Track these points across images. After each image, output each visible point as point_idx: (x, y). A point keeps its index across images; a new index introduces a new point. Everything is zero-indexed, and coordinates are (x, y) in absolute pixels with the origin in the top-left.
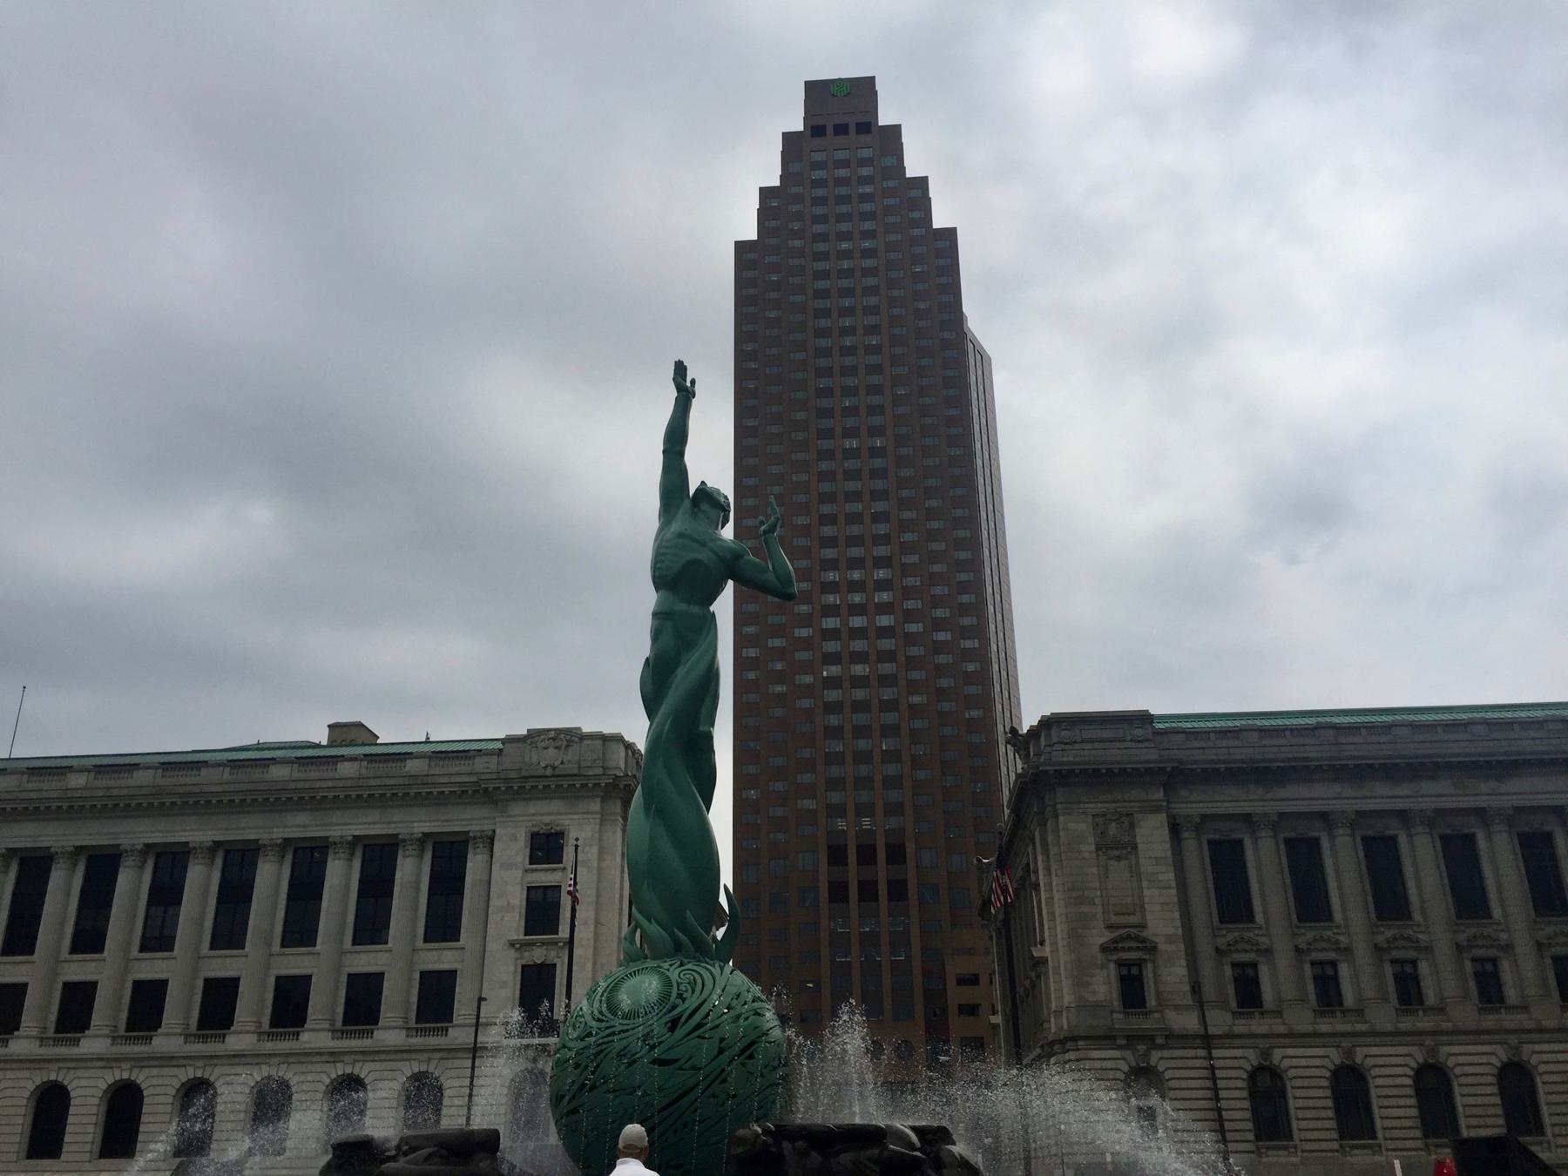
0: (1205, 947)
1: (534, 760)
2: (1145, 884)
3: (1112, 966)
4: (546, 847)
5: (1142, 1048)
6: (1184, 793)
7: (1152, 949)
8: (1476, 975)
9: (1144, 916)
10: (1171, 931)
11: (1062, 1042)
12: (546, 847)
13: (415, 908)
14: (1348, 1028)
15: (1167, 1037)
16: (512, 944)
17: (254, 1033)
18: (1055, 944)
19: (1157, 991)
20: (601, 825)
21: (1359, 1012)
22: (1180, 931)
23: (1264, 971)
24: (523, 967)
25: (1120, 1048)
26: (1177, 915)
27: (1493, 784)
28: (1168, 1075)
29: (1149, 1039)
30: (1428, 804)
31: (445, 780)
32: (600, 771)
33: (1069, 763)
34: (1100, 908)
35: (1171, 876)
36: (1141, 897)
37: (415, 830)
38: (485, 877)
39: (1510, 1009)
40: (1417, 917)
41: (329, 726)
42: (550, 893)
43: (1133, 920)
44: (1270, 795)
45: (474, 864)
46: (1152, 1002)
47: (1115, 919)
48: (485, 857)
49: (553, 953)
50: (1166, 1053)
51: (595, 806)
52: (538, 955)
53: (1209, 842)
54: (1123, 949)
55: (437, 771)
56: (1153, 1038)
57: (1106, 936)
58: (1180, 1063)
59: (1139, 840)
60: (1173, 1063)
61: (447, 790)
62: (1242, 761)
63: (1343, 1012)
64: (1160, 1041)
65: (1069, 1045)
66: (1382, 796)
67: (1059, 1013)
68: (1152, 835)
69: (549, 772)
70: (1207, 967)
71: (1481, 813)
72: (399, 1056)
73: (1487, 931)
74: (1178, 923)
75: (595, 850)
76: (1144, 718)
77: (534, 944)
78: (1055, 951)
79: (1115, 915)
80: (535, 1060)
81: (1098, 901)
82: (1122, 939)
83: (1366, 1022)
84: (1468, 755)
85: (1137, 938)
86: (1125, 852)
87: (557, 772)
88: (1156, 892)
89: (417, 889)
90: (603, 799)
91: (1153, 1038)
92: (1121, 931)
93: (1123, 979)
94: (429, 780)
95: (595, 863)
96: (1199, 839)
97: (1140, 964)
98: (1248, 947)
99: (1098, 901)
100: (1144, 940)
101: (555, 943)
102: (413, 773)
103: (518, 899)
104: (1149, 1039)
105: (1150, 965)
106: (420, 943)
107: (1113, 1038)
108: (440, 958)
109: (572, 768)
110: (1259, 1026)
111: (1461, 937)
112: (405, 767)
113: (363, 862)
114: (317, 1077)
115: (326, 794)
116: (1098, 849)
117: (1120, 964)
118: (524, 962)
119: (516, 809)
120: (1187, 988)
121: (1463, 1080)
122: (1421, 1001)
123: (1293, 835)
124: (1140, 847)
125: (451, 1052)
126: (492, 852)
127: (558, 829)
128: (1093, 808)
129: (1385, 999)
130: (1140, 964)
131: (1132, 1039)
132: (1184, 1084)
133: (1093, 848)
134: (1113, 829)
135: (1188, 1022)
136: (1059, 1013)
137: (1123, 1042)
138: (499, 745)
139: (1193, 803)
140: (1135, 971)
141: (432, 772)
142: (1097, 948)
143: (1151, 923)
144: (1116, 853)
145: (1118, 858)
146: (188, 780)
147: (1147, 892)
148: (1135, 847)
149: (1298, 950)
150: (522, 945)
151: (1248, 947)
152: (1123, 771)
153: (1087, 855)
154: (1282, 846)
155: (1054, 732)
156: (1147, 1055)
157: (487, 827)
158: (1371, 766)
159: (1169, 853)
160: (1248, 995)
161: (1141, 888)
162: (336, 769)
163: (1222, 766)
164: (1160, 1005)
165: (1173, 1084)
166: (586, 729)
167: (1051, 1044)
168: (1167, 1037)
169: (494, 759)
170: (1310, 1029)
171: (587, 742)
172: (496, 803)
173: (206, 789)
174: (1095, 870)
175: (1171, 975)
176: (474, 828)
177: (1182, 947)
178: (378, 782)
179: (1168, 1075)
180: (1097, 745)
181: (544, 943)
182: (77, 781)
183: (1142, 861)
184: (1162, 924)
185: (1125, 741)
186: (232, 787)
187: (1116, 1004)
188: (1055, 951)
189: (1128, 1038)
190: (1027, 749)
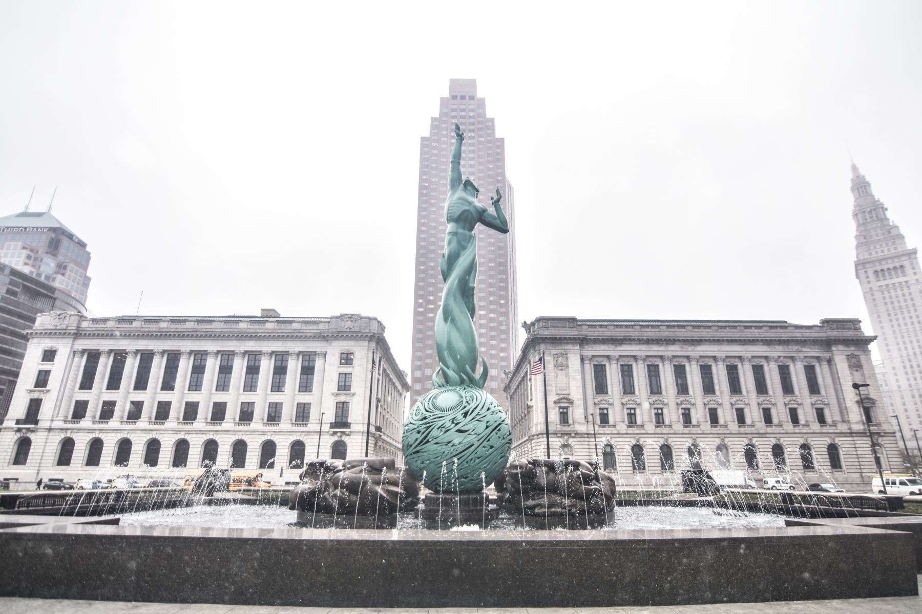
0: (590, 403)
1: (343, 325)
2: (571, 379)
3: (557, 408)
4: (347, 359)
5: (566, 437)
6: (586, 347)
7: (572, 403)
8: (683, 414)
9: (570, 392)
10: (579, 397)
11: (538, 435)
12: (347, 359)
13: (295, 379)
14: (638, 432)
15: (576, 434)
16: (333, 394)
18: (537, 400)
19: (573, 418)
20: (368, 351)
21: (642, 426)
22: (582, 397)
23: (610, 411)
24: (337, 403)
25: (559, 437)
26: (581, 391)
27: (693, 347)
28: (575, 447)
29: (569, 434)
30: (670, 354)
31: (308, 331)
32: (367, 331)
33: (546, 335)
34: (554, 388)
35: (580, 377)
36: (569, 384)
38: (322, 368)
39: (694, 426)
40: (664, 393)
42: (347, 376)
43: (566, 392)
44: (616, 349)
45: (318, 363)
46: (570, 421)
47: (559, 392)
48: (323, 361)
49: (348, 398)
50: (575, 439)
51: (366, 343)
52: (342, 398)
53: (594, 365)
54: (562, 402)
55: (305, 328)
56: (570, 434)
57: (556, 398)
58: (580, 443)
59: (569, 364)
60: (577, 443)
61: (308, 335)
62: (607, 336)
63: (637, 426)
64: (573, 435)
65: (540, 436)
66: (655, 350)
67: (537, 425)
68: (574, 361)
69: (348, 330)
70: (591, 411)
71: (688, 357)
72: (289, 433)
73: (687, 399)
74: (582, 394)
75: (365, 360)
76: (574, 320)
77: (341, 394)
78: (536, 403)
79: (560, 390)
80: (341, 437)
81: (553, 385)
82: (561, 399)
83: (644, 430)
84: (685, 337)
85: (567, 399)
86: (564, 368)
87: (352, 330)
88: (574, 382)
89: (296, 372)
90: (369, 341)
91: (570, 434)
92: (561, 396)
93: (561, 413)
94: (301, 331)
95: (365, 366)
96: (590, 364)
97: (567, 408)
98: (605, 402)
99: (553, 385)
100: (569, 400)
101: (349, 394)
103: (335, 378)
104: (569, 434)
105: (571, 408)
106: (297, 392)
107: (556, 434)
108: (304, 398)
109: (357, 329)
110: (607, 430)
111: (679, 401)
113: (275, 360)
114: (257, 440)
116: (555, 366)
117: (560, 408)
118: (337, 401)
119: (335, 343)
120: (584, 417)
121: (677, 450)
122: (663, 423)
123: (623, 363)
124: (570, 366)
125: (308, 433)
126: (325, 358)
127: (352, 352)
128: (554, 351)
129: (651, 422)
130: (567, 408)
131: (563, 434)
132: (580, 450)
133: (553, 366)
134: (560, 359)
135: (582, 428)
136: (537, 425)
137: (559, 435)
138: (329, 320)
139: (590, 351)
140: (565, 410)
142: (552, 402)
143: (572, 393)
144: (561, 368)
145: (562, 370)
147: (571, 383)
148: (568, 366)
149: (623, 404)
150: (337, 395)
151: (605, 402)
152: (565, 338)
153: (550, 368)
154: (619, 367)
155: (541, 323)
156: (567, 441)
157: (324, 350)
158: (652, 339)
159: (580, 369)
160: (604, 419)
161: (569, 381)
163: (600, 338)
164: (573, 422)
165: (577, 450)
166: (363, 315)
167: (533, 436)
168: (576, 434)
169: (327, 324)
170: (625, 432)
171: (363, 320)
172: (327, 341)
174: (553, 374)
175: (577, 413)
176: (318, 350)
177: (582, 402)
178: (281, 331)
179: (575, 447)
180: (557, 329)
181: (345, 394)
183: (570, 372)
184: (576, 394)
185: (566, 327)
187: (558, 422)
188: (536, 403)
189: (562, 434)
190: (530, 329)
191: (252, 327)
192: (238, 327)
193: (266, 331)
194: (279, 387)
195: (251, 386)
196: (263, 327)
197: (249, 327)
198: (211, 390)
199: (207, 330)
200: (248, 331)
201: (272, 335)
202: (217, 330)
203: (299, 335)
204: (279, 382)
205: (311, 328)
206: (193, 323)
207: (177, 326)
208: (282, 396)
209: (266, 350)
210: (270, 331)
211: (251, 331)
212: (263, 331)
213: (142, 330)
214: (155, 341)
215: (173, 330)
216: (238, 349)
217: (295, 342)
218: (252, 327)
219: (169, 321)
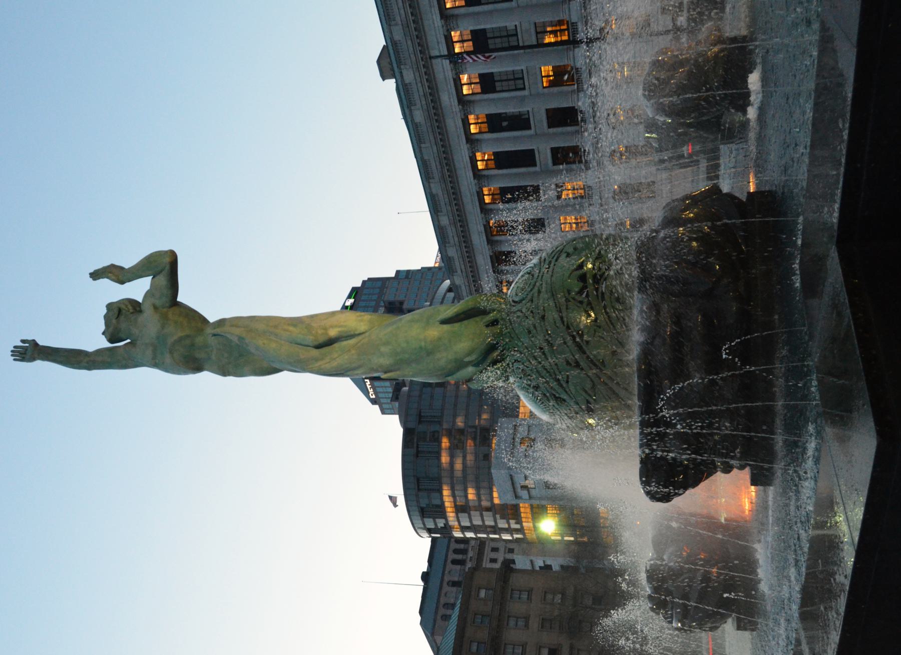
13: (491, 12)
17: (578, 95)
31: (402, 12)
37: (440, 24)
41: (384, 80)
89: (478, 14)
102: (403, 34)
112: (400, 41)
115: (427, 87)
141: (400, 22)
146: (434, 167)
162: (410, 83)
173: (436, 155)
178: (412, 56)
182: (445, 221)
186: (433, 141)
191: (418, 102)
192: (423, 122)
193: (419, 80)
194: (508, 36)
195: (515, 79)
196: (414, 86)
197: (419, 106)
198: (531, 136)
199: (438, 164)
200: (425, 107)
201: (423, 70)
202: (435, 151)
203: (413, 26)
204: (501, 37)
205: (396, 10)
206: (432, 185)
207: (442, 203)
208: (523, 28)
209: (450, 73)
210: (417, 74)
211: (424, 102)
212: (420, 85)
213: (457, 244)
214: (470, 225)
215: (449, 208)
216: (459, 115)
217: (426, 29)
218: (418, 102)
219: (438, 216)
